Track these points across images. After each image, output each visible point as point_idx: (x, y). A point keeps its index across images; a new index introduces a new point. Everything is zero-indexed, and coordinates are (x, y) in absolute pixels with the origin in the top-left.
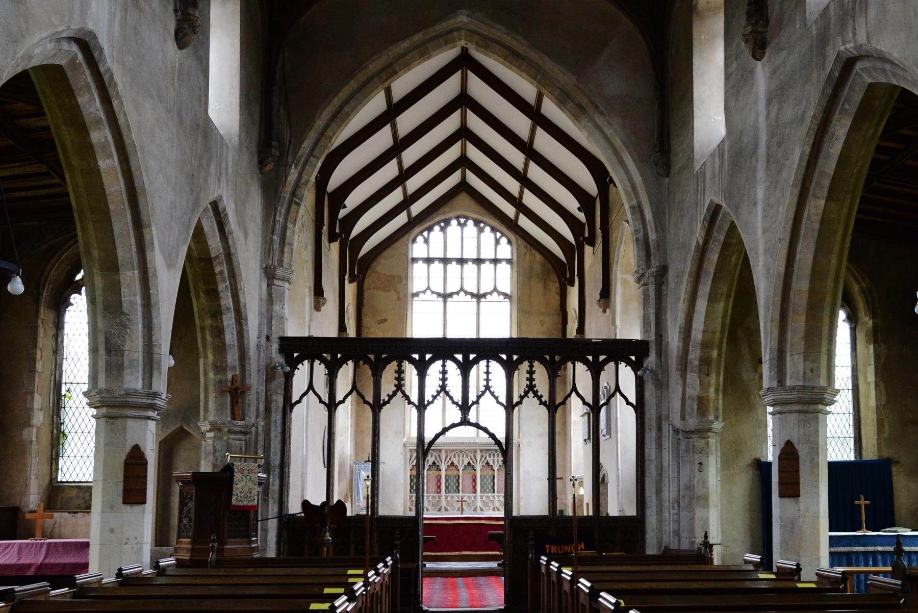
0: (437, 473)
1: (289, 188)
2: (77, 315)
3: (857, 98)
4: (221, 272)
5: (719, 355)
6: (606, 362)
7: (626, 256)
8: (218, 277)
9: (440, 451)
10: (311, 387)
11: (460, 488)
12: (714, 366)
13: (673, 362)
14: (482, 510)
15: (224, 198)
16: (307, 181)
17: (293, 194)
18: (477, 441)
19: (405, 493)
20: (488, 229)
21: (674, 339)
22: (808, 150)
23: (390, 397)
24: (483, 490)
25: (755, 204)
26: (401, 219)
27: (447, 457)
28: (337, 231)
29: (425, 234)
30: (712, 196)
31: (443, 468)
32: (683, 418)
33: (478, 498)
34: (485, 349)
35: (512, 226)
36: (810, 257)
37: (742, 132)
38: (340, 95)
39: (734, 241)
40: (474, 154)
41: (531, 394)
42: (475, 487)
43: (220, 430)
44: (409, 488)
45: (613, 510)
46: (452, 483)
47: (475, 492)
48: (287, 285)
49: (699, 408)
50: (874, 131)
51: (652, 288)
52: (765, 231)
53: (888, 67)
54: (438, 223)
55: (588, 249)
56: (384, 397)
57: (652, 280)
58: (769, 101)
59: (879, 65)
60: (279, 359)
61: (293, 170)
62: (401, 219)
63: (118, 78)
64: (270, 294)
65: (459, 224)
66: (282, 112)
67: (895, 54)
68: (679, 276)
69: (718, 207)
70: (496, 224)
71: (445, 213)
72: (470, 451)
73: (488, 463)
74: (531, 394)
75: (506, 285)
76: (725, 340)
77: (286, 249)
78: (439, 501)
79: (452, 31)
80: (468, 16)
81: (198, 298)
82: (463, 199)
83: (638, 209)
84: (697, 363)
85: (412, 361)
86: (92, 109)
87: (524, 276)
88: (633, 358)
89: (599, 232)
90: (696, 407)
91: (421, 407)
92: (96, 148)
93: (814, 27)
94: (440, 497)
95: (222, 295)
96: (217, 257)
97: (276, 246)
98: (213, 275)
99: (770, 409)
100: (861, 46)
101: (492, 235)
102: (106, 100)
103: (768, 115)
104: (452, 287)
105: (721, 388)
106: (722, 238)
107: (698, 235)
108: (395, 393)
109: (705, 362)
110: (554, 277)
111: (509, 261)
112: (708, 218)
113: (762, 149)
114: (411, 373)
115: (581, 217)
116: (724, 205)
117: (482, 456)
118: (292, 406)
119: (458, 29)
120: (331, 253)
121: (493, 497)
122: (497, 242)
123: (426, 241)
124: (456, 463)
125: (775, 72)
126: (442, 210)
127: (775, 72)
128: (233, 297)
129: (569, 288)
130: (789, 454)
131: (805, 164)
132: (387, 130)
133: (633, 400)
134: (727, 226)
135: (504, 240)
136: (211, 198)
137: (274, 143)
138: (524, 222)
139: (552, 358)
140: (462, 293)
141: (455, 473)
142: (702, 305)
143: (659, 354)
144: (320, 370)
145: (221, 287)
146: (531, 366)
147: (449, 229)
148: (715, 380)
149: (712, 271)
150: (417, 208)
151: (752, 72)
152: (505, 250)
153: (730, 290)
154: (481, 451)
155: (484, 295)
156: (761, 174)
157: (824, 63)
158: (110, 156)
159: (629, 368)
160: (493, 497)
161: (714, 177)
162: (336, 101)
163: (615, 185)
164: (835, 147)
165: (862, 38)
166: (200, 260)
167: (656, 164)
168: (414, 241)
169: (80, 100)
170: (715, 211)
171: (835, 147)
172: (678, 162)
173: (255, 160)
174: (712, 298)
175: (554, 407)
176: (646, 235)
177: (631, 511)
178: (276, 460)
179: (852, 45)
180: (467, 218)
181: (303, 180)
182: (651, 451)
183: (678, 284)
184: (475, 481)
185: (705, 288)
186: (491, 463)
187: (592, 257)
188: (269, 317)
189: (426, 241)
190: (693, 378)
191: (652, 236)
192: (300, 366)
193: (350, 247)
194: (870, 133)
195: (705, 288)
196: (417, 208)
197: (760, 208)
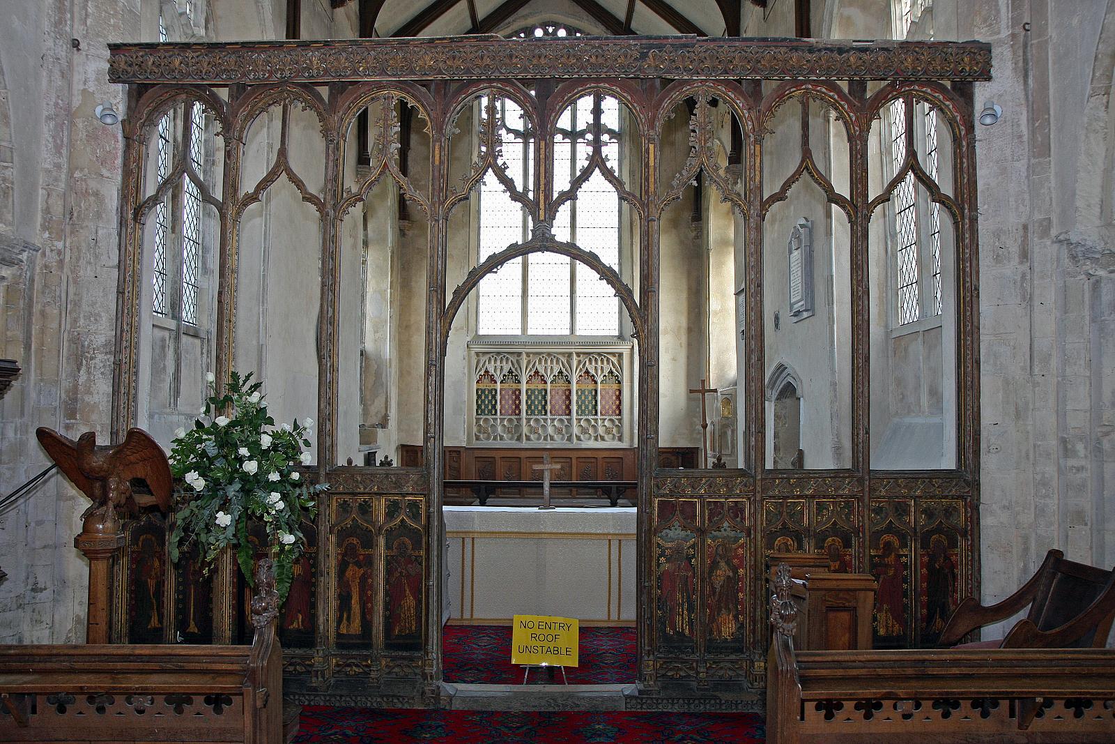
0: (515, 386)
9: (519, 354)
11: (548, 407)
14: (579, 439)
19: (470, 415)
27: (529, 363)
31: (524, 380)
33: (575, 422)
42: (568, 407)
44: (475, 407)
47: (570, 414)
72: (563, 354)
73: (587, 372)
78: (518, 426)
94: (519, 420)
117: (579, 362)
121: (596, 420)
124: (542, 372)
133: (947, 190)
141: (541, 386)
154: (578, 354)
160: (596, 420)
184: (568, 397)
186: (592, 372)
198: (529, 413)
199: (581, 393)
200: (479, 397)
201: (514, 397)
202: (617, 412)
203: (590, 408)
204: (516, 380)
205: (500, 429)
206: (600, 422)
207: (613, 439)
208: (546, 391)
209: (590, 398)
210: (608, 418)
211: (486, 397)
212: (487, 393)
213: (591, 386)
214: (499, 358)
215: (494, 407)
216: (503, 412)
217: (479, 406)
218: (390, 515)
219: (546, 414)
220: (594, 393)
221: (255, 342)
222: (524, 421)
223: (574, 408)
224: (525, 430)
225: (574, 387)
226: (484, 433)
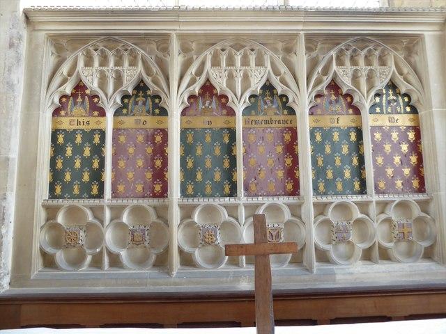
0: (152, 122)
9: (163, 39)
11: (240, 175)
24: (324, 184)
27: (186, 66)
31: (175, 104)
33: (309, 210)
46: (210, 157)
47: (295, 191)
73: (334, 86)
121: (364, 207)
124: (220, 84)
141: (220, 122)
154: (310, 38)
160: (364, 207)
184: (291, 148)
186: (346, 83)
198: (190, 191)
199: (322, 137)
200: (57, 150)
201: (149, 150)
202: (415, 183)
203: (347, 174)
204: (155, 106)
205: (109, 236)
206: (373, 210)
207: (410, 254)
208: (232, 133)
209: (345, 150)
210: (397, 199)
211: (78, 150)
212: (79, 139)
213: (346, 121)
215: (97, 176)
216: (121, 188)
217: (56, 176)
220: (353, 137)
222: (176, 215)
223: (306, 174)
224: (178, 237)
225: (304, 124)
226: (67, 247)
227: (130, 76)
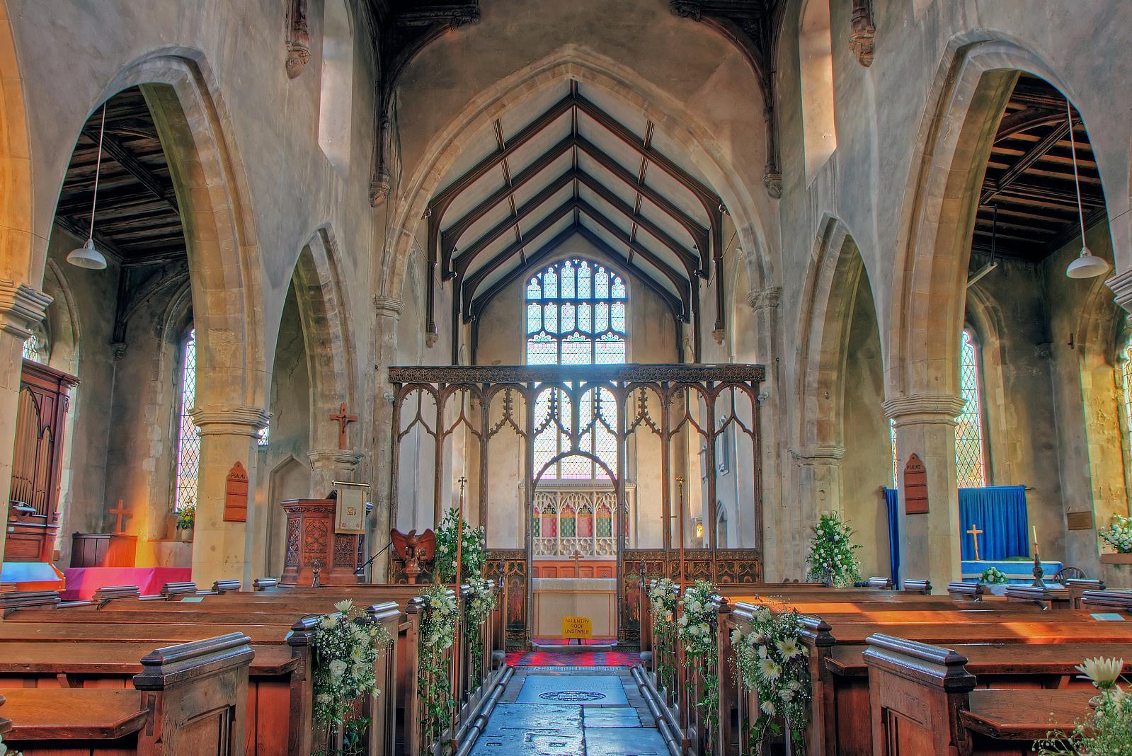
1: (400, 220)
2: (191, 351)
3: (971, 89)
4: (330, 300)
5: (839, 377)
6: (720, 388)
7: (741, 281)
8: (327, 305)
9: (555, 493)
10: (419, 417)
12: (833, 389)
13: (791, 386)
14: (598, 553)
15: (334, 226)
16: (417, 213)
17: (403, 226)
18: (593, 482)
20: (602, 270)
21: (791, 365)
22: (922, 147)
23: (499, 426)
25: (870, 210)
26: (514, 261)
27: (562, 499)
28: (450, 270)
29: (539, 275)
30: (825, 210)
32: (803, 445)
34: (596, 376)
35: (626, 265)
36: (930, 257)
37: (853, 141)
38: (450, 129)
39: (850, 256)
40: (587, 193)
41: (643, 422)
42: (591, 531)
43: (328, 459)
45: (732, 544)
46: (569, 527)
47: (591, 535)
48: (396, 316)
49: (820, 432)
50: (992, 121)
51: (767, 311)
52: (881, 236)
53: (1002, 50)
54: (552, 265)
55: (702, 281)
56: (492, 426)
57: (767, 302)
58: (880, 105)
59: (992, 49)
60: (389, 391)
61: (403, 202)
62: (514, 261)
63: (226, 98)
64: (379, 324)
65: (573, 265)
66: (393, 147)
67: (1009, 33)
68: (794, 296)
69: (832, 221)
70: (610, 264)
71: (558, 255)
72: (587, 493)
73: (604, 505)
74: (643, 422)
75: (620, 325)
76: (845, 362)
77: (396, 280)
79: (559, 65)
80: (575, 49)
81: (308, 327)
82: (577, 239)
83: (750, 232)
84: (815, 385)
85: (520, 389)
86: (201, 129)
87: (637, 317)
88: (749, 383)
89: (713, 262)
90: (816, 432)
91: (529, 435)
92: (204, 167)
93: (922, 23)
94: (555, 540)
95: (330, 323)
96: (326, 285)
97: (387, 277)
98: (322, 303)
99: (893, 421)
100: (972, 31)
101: (606, 275)
102: (215, 119)
103: (878, 119)
104: (568, 326)
105: (842, 412)
106: (838, 254)
107: (813, 253)
108: (503, 423)
109: (824, 384)
110: (669, 316)
111: (623, 301)
112: (822, 233)
113: (875, 154)
114: (518, 398)
115: (697, 252)
116: (838, 217)
118: (400, 436)
119: (565, 63)
120: (445, 290)
122: (611, 282)
123: (541, 283)
125: (884, 74)
126: (557, 251)
127: (884, 74)
128: (342, 325)
129: (685, 324)
130: (915, 470)
131: (919, 161)
132: (499, 168)
133: (750, 427)
134: (841, 241)
135: (618, 280)
136: (320, 224)
137: (384, 177)
138: (639, 260)
139: (665, 384)
140: (576, 334)
141: (571, 516)
142: (819, 324)
143: (777, 377)
144: (427, 397)
145: (330, 315)
146: (643, 393)
147: (563, 270)
148: (835, 402)
149: (828, 288)
150: (529, 249)
151: (859, 80)
152: (619, 291)
153: (848, 308)
155: (599, 335)
156: (874, 179)
157: (934, 56)
158: (218, 175)
159: (745, 393)
161: (826, 190)
162: (446, 135)
163: (727, 212)
164: (950, 141)
165: (973, 24)
166: (310, 288)
167: (767, 185)
168: (529, 283)
169: (189, 120)
170: (830, 224)
171: (950, 141)
172: (789, 181)
173: (367, 193)
174: (829, 318)
175: (671, 434)
176: (759, 257)
177: (750, 544)
178: (384, 491)
179: (963, 32)
180: (581, 259)
181: (413, 213)
182: (769, 479)
183: (794, 304)
185: (822, 305)
187: (706, 289)
188: (377, 347)
189: (541, 283)
190: (811, 401)
191: (766, 258)
192: (408, 396)
193: (464, 288)
194: (988, 125)
195: (822, 305)
196: (529, 249)
197: (874, 213)
205: (541, 547)
214: (541, 496)
218: (510, 570)
219: (574, 535)
221: (412, 490)
224: (560, 547)
227: (546, 502)
